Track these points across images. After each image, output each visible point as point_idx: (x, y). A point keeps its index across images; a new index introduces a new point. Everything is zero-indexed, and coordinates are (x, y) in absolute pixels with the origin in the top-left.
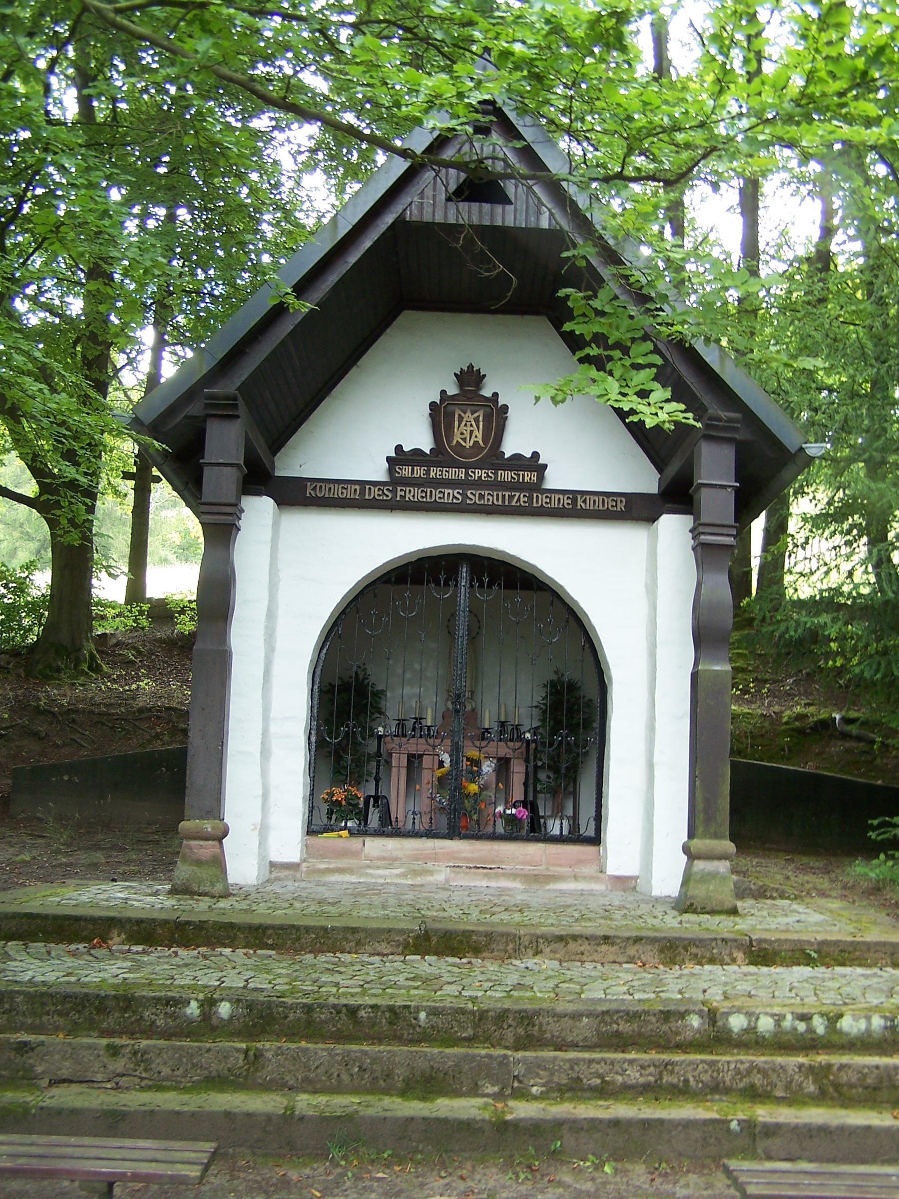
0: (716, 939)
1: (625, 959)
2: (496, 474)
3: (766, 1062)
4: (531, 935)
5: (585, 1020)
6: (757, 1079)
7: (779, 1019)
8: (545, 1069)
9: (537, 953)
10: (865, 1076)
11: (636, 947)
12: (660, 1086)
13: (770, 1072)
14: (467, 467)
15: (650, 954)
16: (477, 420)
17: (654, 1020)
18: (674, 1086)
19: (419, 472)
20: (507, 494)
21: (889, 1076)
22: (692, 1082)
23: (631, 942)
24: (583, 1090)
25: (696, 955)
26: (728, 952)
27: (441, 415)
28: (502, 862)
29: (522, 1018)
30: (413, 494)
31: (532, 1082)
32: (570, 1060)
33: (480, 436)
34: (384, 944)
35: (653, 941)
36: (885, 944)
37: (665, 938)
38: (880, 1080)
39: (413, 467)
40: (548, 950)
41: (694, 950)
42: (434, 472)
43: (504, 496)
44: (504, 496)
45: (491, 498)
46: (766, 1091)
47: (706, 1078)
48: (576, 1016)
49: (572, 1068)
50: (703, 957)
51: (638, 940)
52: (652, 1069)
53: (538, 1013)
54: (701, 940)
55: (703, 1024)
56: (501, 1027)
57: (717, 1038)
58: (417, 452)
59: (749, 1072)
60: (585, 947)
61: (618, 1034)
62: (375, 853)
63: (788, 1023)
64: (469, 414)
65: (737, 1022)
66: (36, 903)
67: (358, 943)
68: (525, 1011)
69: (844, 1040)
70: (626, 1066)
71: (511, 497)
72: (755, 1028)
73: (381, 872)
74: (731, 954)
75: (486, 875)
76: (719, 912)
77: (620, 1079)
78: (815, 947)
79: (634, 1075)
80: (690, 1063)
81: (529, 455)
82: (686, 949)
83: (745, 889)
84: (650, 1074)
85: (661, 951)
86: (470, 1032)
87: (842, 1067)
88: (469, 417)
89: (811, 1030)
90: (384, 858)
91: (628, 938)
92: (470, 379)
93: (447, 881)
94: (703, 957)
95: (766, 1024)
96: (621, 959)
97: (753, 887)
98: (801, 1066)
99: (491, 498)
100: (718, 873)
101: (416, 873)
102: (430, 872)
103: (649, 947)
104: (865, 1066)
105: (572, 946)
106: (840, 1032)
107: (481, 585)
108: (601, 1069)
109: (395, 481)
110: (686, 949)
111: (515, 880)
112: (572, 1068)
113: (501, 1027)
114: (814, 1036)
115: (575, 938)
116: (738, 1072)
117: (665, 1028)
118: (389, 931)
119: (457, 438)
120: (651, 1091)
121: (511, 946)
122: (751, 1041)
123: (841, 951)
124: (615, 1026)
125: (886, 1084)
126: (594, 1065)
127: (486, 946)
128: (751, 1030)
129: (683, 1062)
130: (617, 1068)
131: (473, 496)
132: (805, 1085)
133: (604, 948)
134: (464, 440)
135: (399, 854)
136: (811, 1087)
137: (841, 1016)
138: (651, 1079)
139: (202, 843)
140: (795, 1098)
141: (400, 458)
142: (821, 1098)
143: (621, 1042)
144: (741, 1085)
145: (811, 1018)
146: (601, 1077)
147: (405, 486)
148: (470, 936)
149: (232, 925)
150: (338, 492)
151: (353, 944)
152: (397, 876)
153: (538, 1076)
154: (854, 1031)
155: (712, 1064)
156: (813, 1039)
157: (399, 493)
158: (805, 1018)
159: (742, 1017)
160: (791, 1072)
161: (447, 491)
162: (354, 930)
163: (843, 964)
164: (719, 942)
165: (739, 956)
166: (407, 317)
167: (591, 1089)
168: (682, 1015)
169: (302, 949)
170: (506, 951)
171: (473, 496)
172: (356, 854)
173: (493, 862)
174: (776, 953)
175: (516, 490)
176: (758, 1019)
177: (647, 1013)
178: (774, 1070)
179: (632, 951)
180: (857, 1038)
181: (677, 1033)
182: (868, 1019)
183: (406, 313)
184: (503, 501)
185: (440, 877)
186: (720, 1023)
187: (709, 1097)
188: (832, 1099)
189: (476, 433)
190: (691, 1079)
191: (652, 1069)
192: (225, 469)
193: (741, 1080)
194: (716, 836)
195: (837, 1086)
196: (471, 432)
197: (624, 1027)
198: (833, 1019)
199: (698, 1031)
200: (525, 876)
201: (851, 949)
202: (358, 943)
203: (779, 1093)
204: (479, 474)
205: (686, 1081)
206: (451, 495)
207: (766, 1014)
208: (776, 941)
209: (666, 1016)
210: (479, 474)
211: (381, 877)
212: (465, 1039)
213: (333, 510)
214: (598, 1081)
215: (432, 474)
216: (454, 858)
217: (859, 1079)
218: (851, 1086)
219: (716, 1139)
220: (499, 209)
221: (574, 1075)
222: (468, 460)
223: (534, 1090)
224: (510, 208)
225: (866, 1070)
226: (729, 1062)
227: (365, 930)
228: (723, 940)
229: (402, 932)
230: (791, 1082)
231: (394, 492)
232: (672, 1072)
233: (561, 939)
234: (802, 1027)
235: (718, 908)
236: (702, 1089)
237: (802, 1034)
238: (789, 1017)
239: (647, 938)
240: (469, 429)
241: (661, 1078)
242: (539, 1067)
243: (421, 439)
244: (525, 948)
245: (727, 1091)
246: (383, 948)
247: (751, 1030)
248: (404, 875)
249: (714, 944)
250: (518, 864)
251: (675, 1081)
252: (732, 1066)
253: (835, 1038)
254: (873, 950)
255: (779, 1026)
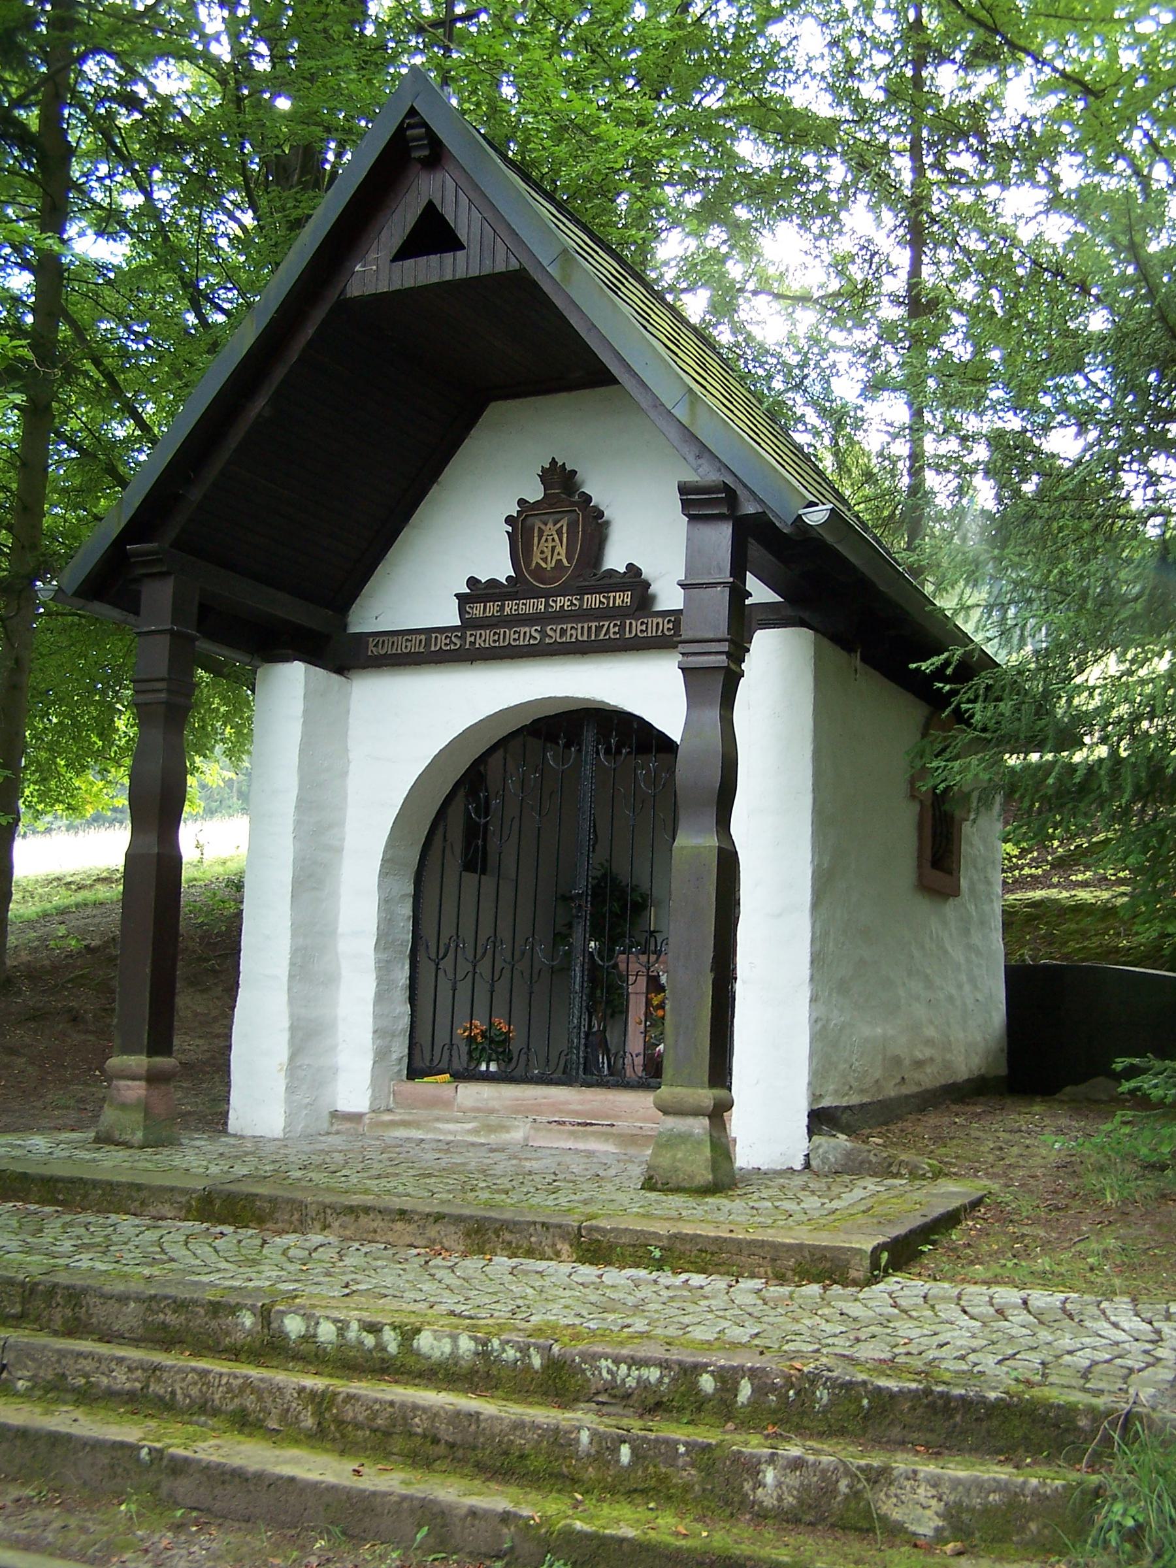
0: (535, 1223)
1: (424, 1243)
2: (581, 600)
3: (262, 1380)
4: (318, 1203)
5: (132, 1305)
6: (250, 1401)
7: (342, 1327)
8: (34, 1360)
9: (325, 1227)
10: (375, 1415)
11: (438, 1227)
12: (145, 1396)
13: (265, 1395)
14: (547, 595)
15: (452, 1237)
16: (559, 532)
17: (202, 1312)
18: (161, 1398)
19: (492, 608)
20: (594, 624)
21: (404, 1418)
22: (179, 1397)
23: (431, 1219)
24: (66, 1391)
25: (510, 1243)
26: (549, 1241)
27: (521, 530)
28: (618, 1117)
29: (70, 1295)
30: (485, 639)
31: (19, 1374)
32: (58, 1351)
33: (563, 552)
34: (167, 1206)
35: (458, 1219)
36: (763, 1244)
37: (471, 1217)
38: (393, 1420)
39: (485, 603)
40: (337, 1224)
41: (508, 1236)
42: (510, 607)
43: (590, 628)
44: (590, 628)
45: (576, 632)
46: (259, 1420)
47: (194, 1392)
48: (123, 1299)
49: (59, 1361)
50: (519, 1247)
51: (439, 1218)
52: (139, 1373)
53: (85, 1291)
54: (515, 1223)
55: (254, 1324)
56: (50, 1306)
57: (271, 1347)
58: (493, 582)
59: (242, 1389)
60: (378, 1224)
61: (164, 1326)
62: (469, 1103)
63: (352, 1334)
64: (550, 525)
65: (294, 1326)
66: (121, 1153)
67: (143, 1203)
68: (73, 1287)
69: (423, 1365)
70: (113, 1365)
71: (599, 629)
72: (315, 1336)
73: (451, 1126)
74: (554, 1245)
75: (572, 1133)
76: (678, 1190)
77: (105, 1381)
78: (665, 1243)
79: (121, 1380)
80: (180, 1370)
81: (622, 570)
82: (497, 1233)
83: (862, 1163)
84: (137, 1380)
85: (468, 1235)
86: (16, 1309)
87: (350, 1398)
88: (550, 529)
89: (381, 1347)
90: (478, 1110)
91: (428, 1215)
92: (561, 482)
93: (526, 1139)
94: (519, 1247)
95: (326, 1332)
96: (419, 1241)
97: (874, 1159)
98: (302, 1390)
99: (576, 632)
100: (691, 1135)
101: (490, 1129)
102: (507, 1129)
103: (453, 1229)
104: (376, 1401)
105: (364, 1220)
106: (418, 1354)
107: (608, 752)
108: (87, 1365)
109: (468, 624)
110: (497, 1233)
111: (607, 1140)
112: (59, 1361)
113: (50, 1306)
114: (385, 1356)
115: (367, 1210)
116: (229, 1388)
117: (214, 1324)
118: (172, 1189)
119: (537, 559)
120: (135, 1402)
121: (296, 1216)
122: (308, 1355)
123: (701, 1250)
124: (161, 1316)
125: (399, 1429)
126: (81, 1360)
127: (272, 1213)
128: (309, 1338)
129: (173, 1367)
130: (103, 1367)
131: (553, 633)
132: (302, 1417)
133: (399, 1226)
134: (545, 560)
135: (495, 1104)
136: (309, 1422)
137: (418, 1331)
138: (138, 1385)
139: (129, 1083)
140: (286, 1433)
141: (478, 592)
142: (318, 1437)
143: (167, 1339)
144: (231, 1407)
145: (380, 1330)
146: (86, 1376)
147: (487, 628)
148: (254, 1201)
149: (25, 1175)
150: (404, 647)
151: (137, 1204)
152: (469, 1132)
153: (26, 1367)
154: (437, 1354)
155: (204, 1373)
156: (383, 1360)
157: (469, 639)
158: (373, 1328)
159: (298, 1318)
160: (289, 1397)
161: (523, 630)
162: (139, 1187)
163: (702, 1271)
164: (539, 1227)
165: (565, 1248)
166: (495, 411)
167: (75, 1390)
168: (234, 1309)
169: (90, 1208)
170: (291, 1223)
171: (553, 633)
172: (448, 1104)
173: (607, 1117)
174: (611, 1247)
175: (604, 618)
176: (317, 1323)
177: (195, 1302)
178: (270, 1392)
179: (432, 1231)
180: (440, 1365)
181: (228, 1334)
182: (454, 1338)
183: (493, 404)
184: (589, 636)
185: (517, 1136)
186: (274, 1325)
187: (195, 1418)
188: (334, 1440)
189: (558, 549)
190: (179, 1391)
191: (139, 1373)
192: (158, 637)
193: (232, 1399)
194: (690, 1084)
195: (340, 1423)
196: (553, 548)
197: (171, 1318)
198: (409, 1334)
199: (250, 1333)
200: (620, 1135)
201: (714, 1248)
202: (143, 1203)
203: (273, 1424)
204: (562, 602)
205: (173, 1393)
206: (530, 634)
207: (327, 1318)
208: (612, 1230)
209: (216, 1308)
210: (562, 602)
211: (450, 1132)
212: (13, 1316)
213: (409, 670)
214: (83, 1381)
215: (507, 609)
216: (561, 1111)
217: (367, 1418)
218: (358, 1426)
219: (125, 1469)
220: (448, 257)
221: (60, 1371)
222: (563, 586)
223: (20, 1384)
224: (460, 254)
225: (377, 1407)
226: (221, 1375)
227: (149, 1188)
228: (543, 1224)
229: (184, 1191)
230: (288, 1410)
231: (462, 638)
232: (159, 1380)
233: (351, 1210)
234: (370, 1340)
235: (686, 1184)
236: (190, 1407)
237: (370, 1351)
238: (355, 1325)
239: (450, 1216)
240: (550, 545)
241: (147, 1386)
242: (28, 1355)
243: (501, 569)
244: (313, 1219)
245: (216, 1412)
246: (166, 1210)
247: (309, 1338)
248: (475, 1131)
249: (532, 1229)
250: (638, 1120)
251: (162, 1391)
252: (224, 1381)
253: (411, 1361)
254: (745, 1252)
255: (343, 1336)
